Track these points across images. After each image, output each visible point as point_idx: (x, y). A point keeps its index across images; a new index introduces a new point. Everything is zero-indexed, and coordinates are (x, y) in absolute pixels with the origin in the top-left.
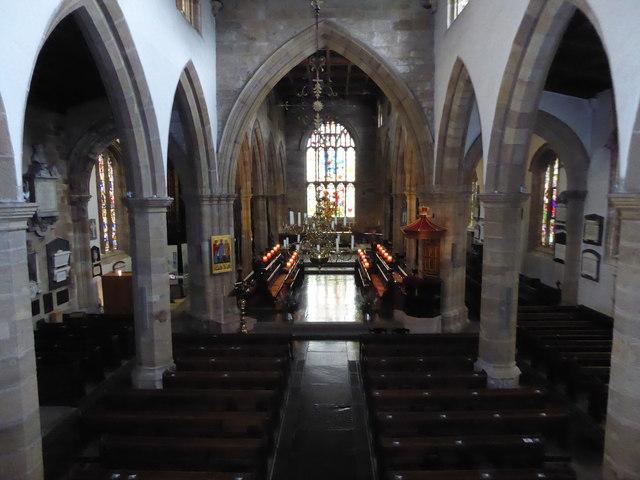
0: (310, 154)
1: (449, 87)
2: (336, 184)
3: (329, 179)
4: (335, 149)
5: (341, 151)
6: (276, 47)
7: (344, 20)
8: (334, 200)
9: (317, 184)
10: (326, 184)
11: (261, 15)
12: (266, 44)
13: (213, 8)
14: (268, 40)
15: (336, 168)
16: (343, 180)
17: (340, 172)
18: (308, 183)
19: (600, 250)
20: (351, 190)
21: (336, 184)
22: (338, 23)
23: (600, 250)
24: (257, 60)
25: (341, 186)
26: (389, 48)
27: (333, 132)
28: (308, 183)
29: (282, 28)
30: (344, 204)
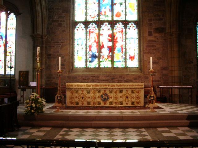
2: (113, 23)
3: (102, 18)
8: (110, 44)
9: (86, 24)
10: (99, 23)
16: (122, 18)
18: (77, 23)
20: (133, 32)
21: (113, 23)
25: (120, 26)
28: (77, 23)
30: (124, 49)
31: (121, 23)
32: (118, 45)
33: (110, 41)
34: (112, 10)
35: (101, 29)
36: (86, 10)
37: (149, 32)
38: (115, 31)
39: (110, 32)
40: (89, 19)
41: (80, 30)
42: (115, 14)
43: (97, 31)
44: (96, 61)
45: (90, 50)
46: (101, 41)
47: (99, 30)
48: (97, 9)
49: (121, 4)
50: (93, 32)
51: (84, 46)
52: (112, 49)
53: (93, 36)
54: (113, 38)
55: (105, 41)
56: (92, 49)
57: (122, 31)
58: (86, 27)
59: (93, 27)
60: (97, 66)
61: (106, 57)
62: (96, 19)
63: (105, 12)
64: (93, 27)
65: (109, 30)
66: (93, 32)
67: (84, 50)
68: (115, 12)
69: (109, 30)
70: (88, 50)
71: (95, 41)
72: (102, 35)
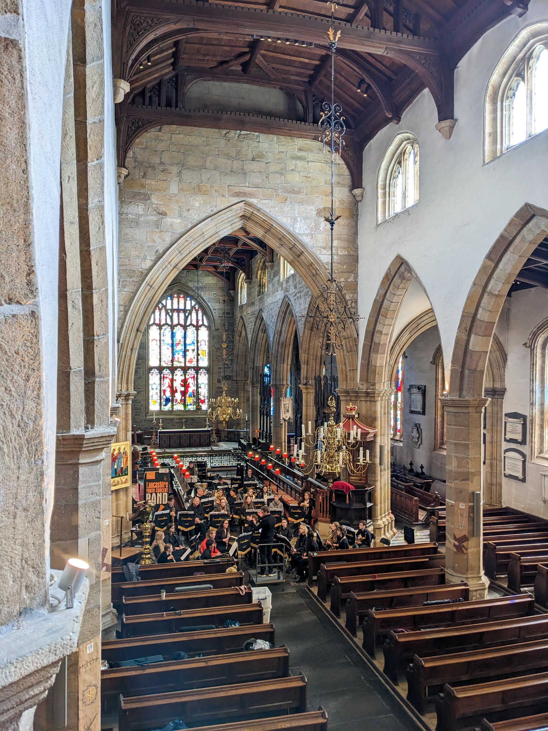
0: (154, 332)
1: (383, 283)
2: (185, 369)
3: (176, 364)
4: (185, 327)
5: (191, 331)
6: (190, 226)
7: (266, 201)
9: (160, 369)
11: (174, 188)
12: (179, 220)
13: (119, 176)
14: (180, 216)
15: (185, 351)
16: (194, 364)
17: (191, 355)
19: (525, 449)
21: (185, 369)
22: (259, 206)
23: (525, 449)
24: (168, 239)
25: (192, 372)
26: (312, 235)
27: (182, 307)
28: (151, 368)
29: (197, 204)
30: (196, 394)
31: (193, 370)
32: (190, 390)
33: (182, 386)
34: (185, 356)
35: (175, 374)
36: (160, 355)
37: (218, 379)
38: (187, 377)
39: (183, 378)
40: (163, 364)
41: (154, 375)
42: (187, 360)
43: (171, 377)
44: (170, 404)
45: (164, 394)
46: (174, 386)
47: (173, 376)
48: (171, 355)
49: (193, 350)
50: (166, 378)
51: (158, 391)
52: (184, 393)
53: (167, 382)
54: (185, 383)
55: (177, 384)
56: (166, 393)
57: (194, 377)
58: (160, 373)
59: (166, 372)
60: (171, 409)
61: (179, 401)
62: (170, 364)
63: (178, 358)
64: (166, 372)
65: (182, 375)
66: (166, 378)
67: (159, 394)
68: (188, 358)
69: (182, 375)
70: (162, 394)
71: (169, 386)
72: (175, 380)
